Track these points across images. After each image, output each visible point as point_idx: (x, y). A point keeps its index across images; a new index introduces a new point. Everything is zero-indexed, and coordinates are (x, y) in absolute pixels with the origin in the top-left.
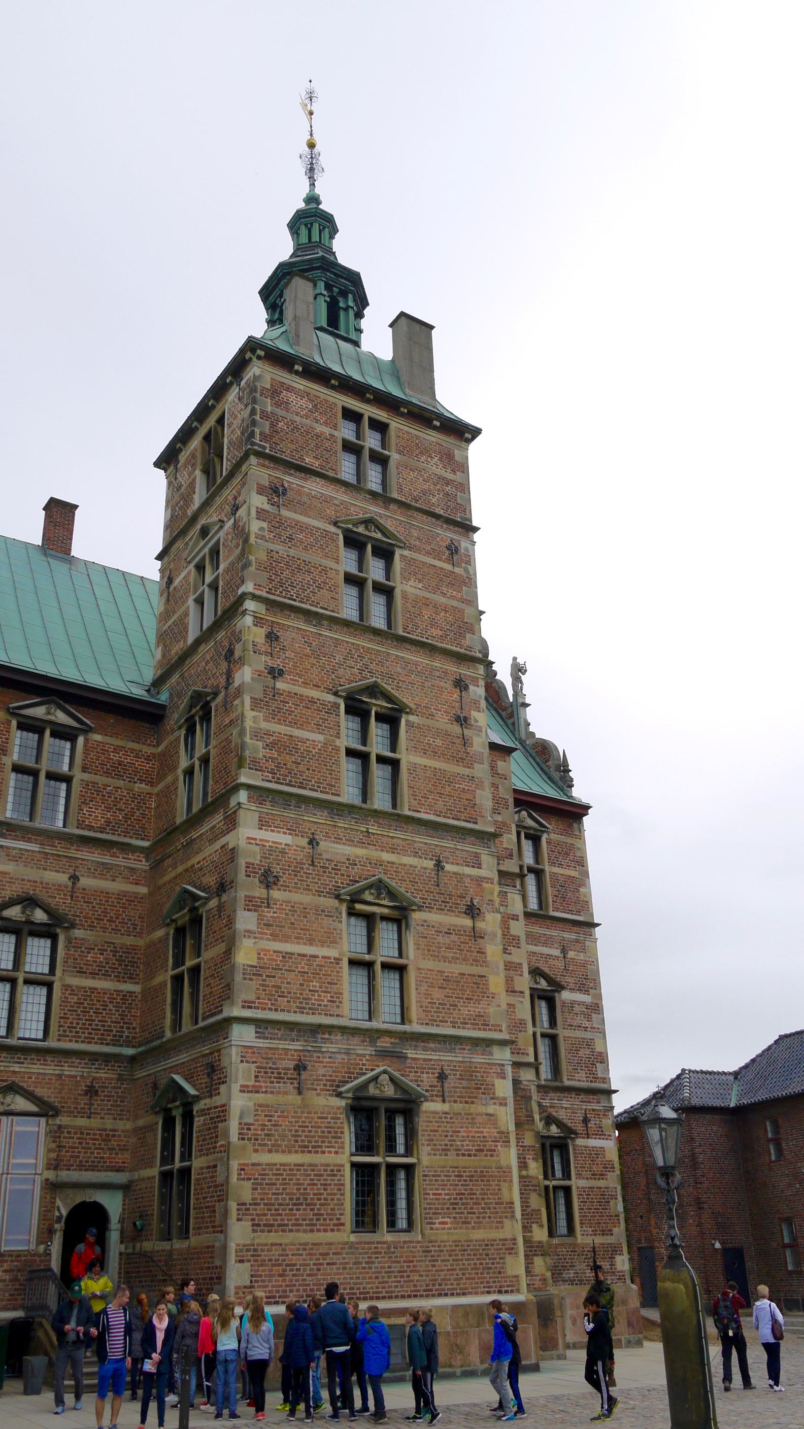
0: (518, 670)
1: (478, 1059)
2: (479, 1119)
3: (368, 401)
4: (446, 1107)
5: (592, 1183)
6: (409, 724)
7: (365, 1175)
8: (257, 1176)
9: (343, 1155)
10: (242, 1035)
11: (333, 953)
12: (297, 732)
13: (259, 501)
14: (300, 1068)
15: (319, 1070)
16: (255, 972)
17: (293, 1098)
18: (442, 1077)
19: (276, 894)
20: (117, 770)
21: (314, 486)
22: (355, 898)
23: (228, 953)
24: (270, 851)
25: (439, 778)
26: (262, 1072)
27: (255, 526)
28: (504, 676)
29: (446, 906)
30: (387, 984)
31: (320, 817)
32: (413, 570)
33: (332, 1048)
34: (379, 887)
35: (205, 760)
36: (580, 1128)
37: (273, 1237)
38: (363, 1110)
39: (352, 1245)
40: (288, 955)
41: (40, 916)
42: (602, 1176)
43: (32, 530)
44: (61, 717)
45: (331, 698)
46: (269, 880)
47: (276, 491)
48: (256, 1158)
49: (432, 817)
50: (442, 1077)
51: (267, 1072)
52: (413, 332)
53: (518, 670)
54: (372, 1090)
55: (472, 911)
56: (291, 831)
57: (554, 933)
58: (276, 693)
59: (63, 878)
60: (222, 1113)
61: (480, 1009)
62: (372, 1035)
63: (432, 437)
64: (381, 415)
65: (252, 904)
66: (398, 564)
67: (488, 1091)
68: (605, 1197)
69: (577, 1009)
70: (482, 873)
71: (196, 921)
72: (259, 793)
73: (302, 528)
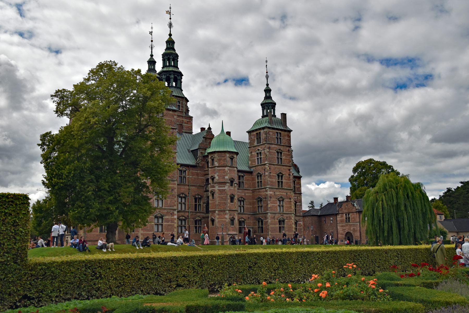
7: (280, 227)
8: (272, 228)
9: (278, 226)
10: (269, 214)
15: (276, 217)
16: (270, 207)
20: (248, 180)
21: (273, 146)
25: (287, 183)
26: (271, 218)
30: (282, 208)
31: (275, 190)
32: (285, 155)
34: (281, 197)
35: (261, 181)
38: (280, 221)
44: (242, 174)
46: (271, 197)
47: (269, 148)
52: (284, 115)
55: (290, 199)
60: (267, 222)
62: (280, 213)
63: (286, 133)
64: (280, 132)
65: (269, 200)
68: (301, 229)
73: (272, 152)
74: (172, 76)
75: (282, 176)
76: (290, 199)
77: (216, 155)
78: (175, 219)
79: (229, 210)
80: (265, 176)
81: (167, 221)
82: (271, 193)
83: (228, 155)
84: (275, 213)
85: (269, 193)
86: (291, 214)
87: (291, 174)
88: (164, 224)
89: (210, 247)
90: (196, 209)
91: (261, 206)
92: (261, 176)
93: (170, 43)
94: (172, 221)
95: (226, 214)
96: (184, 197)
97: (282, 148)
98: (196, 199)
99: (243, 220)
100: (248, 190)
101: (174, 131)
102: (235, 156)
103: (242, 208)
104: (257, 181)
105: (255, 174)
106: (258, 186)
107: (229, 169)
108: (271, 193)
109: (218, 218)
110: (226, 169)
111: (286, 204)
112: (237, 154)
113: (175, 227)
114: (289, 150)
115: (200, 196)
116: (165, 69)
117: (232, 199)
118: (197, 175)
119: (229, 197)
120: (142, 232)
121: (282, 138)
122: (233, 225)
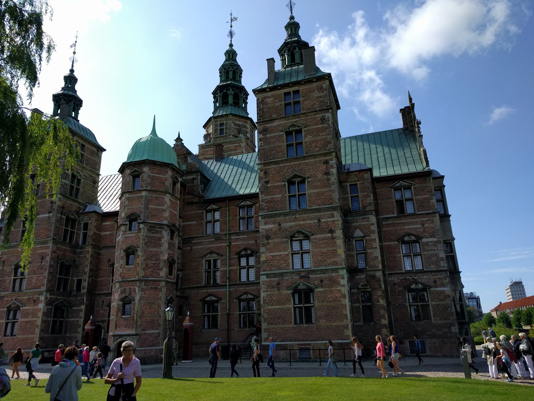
1: (334, 274)
2: (334, 292)
3: (291, 87)
4: (323, 289)
5: (439, 303)
6: (308, 182)
11: (286, 253)
12: (274, 196)
14: (279, 284)
16: (265, 262)
17: (277, 292)
18: (322, 281)
19: (270, 241)
21: (276, 123)
22: (292, 237)
24: (267, 231)
29: (322, 232)
33: (287, 278)
34: (299, 232)
36: (432, 284)
37: (273, 326)
39: (294, 328)
40: (274, 256)
42: (444, 300)
44: (248, 203)
45: (283, 183)
48: (268, 308)
49: (316, 207)
50: (322, 281)
51: (270, 286)
54: (299, 287)
55: (332, 231)
56: (273, 223)
57: (418, 220)
58: (268, 187)
59: (253, 242)
61: (334, 260)
62: (298, 273)
63: (314, 85)
64: (295, 88)
65: (264, 245)
67: (338, 284)
69: (430, 244)
70: (335, 219)
72: (264, 217)
73: (272, 137)
75: (303, 181)
76: (332, 231)
78: (40, 309)
79: (120, 282)
82: (271, 226)
84: (282, 274)
93: (231, 54)
94: (34, 315)
97: (300, 121)
102: (146, 169)
107: (128, 199)
108: (271, 226)
113: (37, 326)
114: (323, 120)
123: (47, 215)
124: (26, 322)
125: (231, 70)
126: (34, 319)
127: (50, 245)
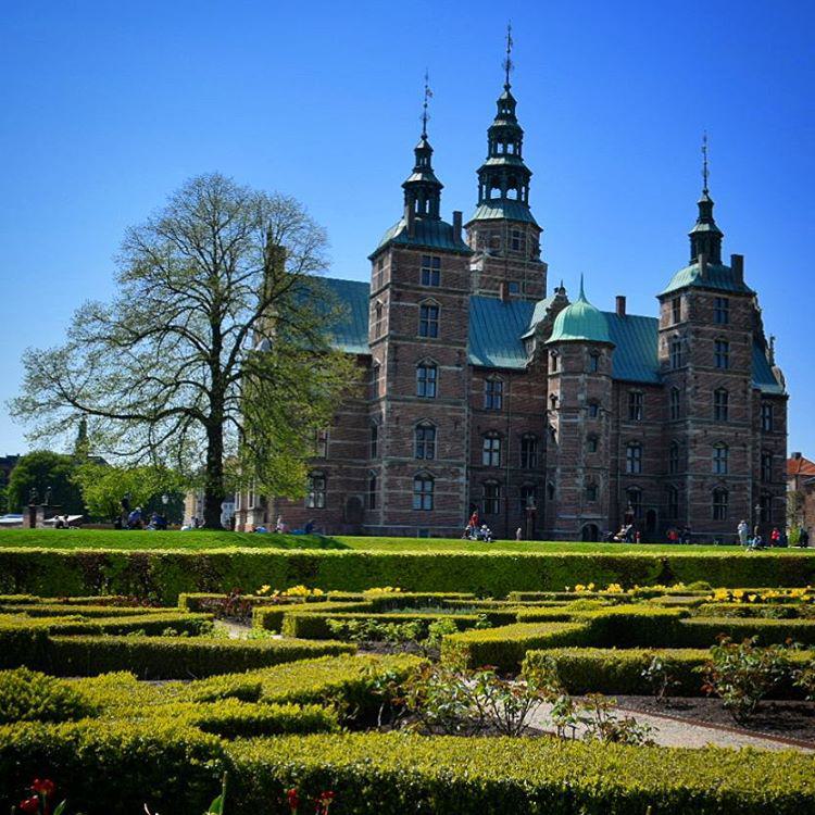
0: (772, 338)
7: (716, 507)
10: (690, 478)
13: (692, 337)
21: (706, 328)
23: (687, 458)
27: (691, 345)
28: (767, 338)
31: (707, 426)
41: (637, 444)
43: (613, 309)
47: (697, 333)
52: (738, 260)
53: (772, 338)
55: (744, 446)
63: (742, 299)
64: (726, 296)
66: (730, 348)
71: (676, 448)
74: (504, 177)
75: (726, 396)
77: (562, 347)
78: (462, 484)
80: (685, 394)
81: (444, 487)
82: (697, 431)
83: (586, 349)
85: (693, 431)
86: (745, 479)
87: (750, 391)
88: (436, 493)
89: (395, 543)
90: (524, 466)
91: (676, 461)
92: (678, 392)
95: (576, 476)
96: (496, 438)
98: (524, 442)
99: (636, 488)
100: (651, 424)
101: (464, 297)
102: (604, 351)
103: (722, 463)
104: (671, 405)
105: (668, 390)
106: (673, 417)
107: (589, 381)
109: (560, 486)
110: (581, 378)
111: (733, 455)
112: (610, 346)
113: (461, 502)
115: (533, 437)
116: (493, 162)
117: (593, 439)
118: (529, 389)
119: (584, 440)
120: (386, 509)
121: (730, 310)
122: (594, 499)
123: (456, 368)
124: (445, 496)
125: (506, 133)
126: (457, 494)
127: (466, 408)
